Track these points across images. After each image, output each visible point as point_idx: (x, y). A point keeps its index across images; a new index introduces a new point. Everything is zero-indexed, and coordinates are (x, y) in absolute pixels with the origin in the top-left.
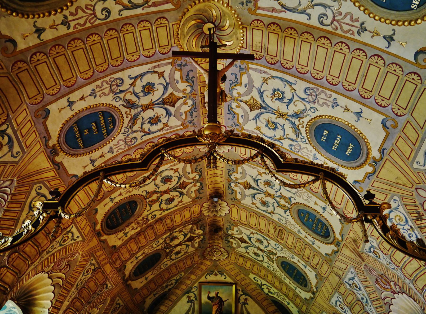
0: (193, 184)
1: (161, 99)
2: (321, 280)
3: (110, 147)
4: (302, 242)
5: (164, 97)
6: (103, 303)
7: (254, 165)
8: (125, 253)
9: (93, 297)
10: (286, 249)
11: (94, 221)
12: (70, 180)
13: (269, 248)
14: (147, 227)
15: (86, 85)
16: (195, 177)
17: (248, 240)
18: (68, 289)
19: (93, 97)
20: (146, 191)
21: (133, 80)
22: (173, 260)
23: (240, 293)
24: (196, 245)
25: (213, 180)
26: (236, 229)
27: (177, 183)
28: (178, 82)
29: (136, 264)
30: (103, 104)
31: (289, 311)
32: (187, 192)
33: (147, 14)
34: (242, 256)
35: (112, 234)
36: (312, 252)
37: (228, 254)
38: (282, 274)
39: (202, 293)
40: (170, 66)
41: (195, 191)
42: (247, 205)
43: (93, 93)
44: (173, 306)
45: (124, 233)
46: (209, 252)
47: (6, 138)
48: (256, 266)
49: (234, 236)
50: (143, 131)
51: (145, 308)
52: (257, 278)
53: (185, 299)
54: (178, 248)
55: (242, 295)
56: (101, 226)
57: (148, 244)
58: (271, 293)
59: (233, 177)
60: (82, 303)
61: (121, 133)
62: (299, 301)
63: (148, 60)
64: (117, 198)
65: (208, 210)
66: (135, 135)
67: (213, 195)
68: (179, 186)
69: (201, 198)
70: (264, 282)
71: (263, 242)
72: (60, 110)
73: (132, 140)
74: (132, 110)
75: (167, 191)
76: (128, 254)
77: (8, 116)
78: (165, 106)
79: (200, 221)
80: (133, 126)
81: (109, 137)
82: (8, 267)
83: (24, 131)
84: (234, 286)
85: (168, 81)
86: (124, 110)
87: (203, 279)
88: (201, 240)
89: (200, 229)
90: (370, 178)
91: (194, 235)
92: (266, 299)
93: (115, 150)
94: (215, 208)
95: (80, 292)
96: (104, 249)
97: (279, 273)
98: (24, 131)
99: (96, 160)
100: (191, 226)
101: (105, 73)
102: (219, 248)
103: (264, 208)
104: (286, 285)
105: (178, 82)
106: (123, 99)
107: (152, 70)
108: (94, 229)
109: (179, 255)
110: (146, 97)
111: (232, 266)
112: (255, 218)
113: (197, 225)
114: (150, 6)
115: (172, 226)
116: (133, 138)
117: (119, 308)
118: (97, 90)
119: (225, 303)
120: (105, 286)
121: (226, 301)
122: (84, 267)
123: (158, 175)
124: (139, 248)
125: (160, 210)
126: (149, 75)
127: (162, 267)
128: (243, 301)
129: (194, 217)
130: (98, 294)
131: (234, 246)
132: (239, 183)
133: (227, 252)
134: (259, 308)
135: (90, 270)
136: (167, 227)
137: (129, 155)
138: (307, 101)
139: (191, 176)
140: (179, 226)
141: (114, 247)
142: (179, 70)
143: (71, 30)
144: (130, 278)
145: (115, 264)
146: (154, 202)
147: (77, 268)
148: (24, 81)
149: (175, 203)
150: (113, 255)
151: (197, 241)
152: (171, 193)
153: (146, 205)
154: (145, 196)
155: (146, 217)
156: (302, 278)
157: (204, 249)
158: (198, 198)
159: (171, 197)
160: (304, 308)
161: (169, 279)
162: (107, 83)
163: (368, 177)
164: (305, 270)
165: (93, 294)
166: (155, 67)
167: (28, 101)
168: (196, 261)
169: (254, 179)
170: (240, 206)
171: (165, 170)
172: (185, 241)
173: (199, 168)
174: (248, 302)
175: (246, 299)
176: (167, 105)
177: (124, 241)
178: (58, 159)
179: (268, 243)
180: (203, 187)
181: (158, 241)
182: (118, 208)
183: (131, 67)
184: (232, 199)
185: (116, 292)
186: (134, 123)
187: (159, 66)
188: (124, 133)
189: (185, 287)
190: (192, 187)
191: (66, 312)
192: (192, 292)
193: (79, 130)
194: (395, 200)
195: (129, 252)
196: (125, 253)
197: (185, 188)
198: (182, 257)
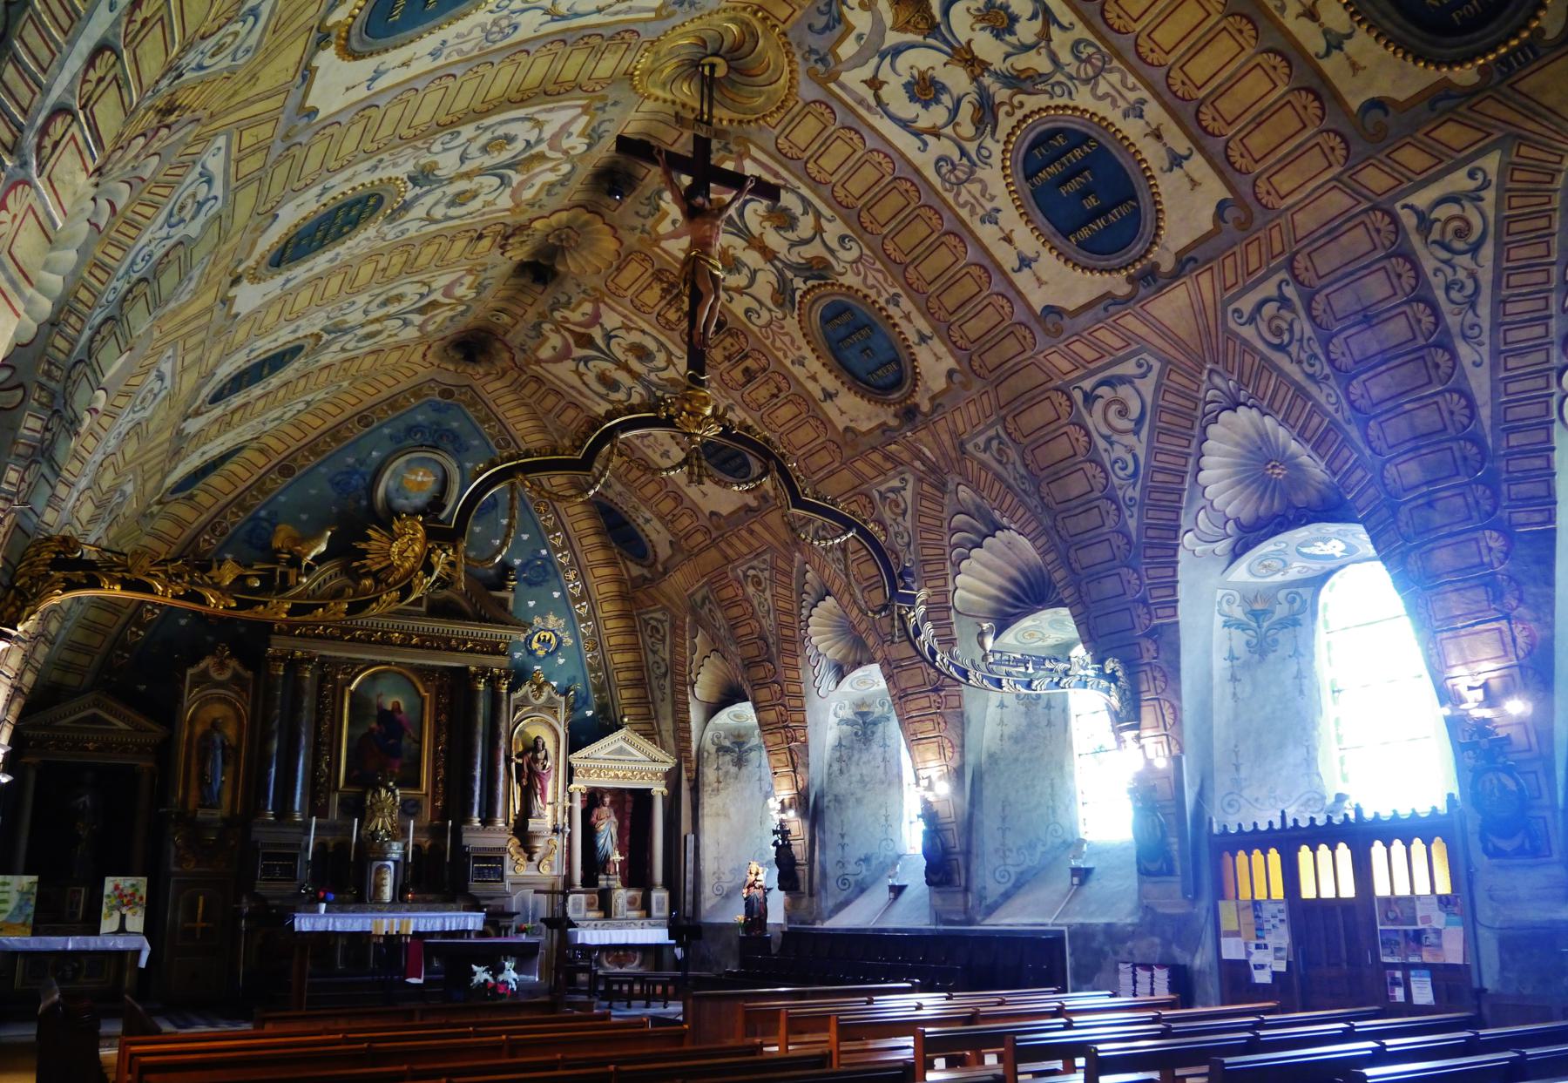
1: (930, 41)
3: (1126, 115)
5: (920, 38)
12: (1231, 225)
15: (978, 240)
21: (926, 137)
28: (860, 37)
30: (1007, 185)
33: (799, 179)
40: (844, 77)
43: (991, 218)
50: (1045, 36)
61: (1071, 104)
63: (865, 132)
66: (1065, 57)
73: (1084, 56)
74: (997, 100)
77: (1057, 389)
78: (938, 18)
80: (1040, 75)
81: (1094, 134)
82: (1389, 460)
83: (1089, 354)
85: (876, 60)
86: (1005, 124)
93: (1132, 96)
98: (1089, 354)
99: (1170, 151)
101: (938, 208)
105: (860, 37)
108: (1471, 92)
110: (948, 83)
116: (1077, 58)
118: (980, 211)
126: (892, 108)
137: (1136, 45)
142: (836, 56)
143: (898, 290)
148: (997, 361)
162: (958, 194)
166: (869, 108)
167: (1029, 354)
176: (932, 17)
178: (1167, 265)
183: (902, 155)
186: (1030, 77)
187: (861, 102)
188: (1070, 93)
193: (1085, 224)
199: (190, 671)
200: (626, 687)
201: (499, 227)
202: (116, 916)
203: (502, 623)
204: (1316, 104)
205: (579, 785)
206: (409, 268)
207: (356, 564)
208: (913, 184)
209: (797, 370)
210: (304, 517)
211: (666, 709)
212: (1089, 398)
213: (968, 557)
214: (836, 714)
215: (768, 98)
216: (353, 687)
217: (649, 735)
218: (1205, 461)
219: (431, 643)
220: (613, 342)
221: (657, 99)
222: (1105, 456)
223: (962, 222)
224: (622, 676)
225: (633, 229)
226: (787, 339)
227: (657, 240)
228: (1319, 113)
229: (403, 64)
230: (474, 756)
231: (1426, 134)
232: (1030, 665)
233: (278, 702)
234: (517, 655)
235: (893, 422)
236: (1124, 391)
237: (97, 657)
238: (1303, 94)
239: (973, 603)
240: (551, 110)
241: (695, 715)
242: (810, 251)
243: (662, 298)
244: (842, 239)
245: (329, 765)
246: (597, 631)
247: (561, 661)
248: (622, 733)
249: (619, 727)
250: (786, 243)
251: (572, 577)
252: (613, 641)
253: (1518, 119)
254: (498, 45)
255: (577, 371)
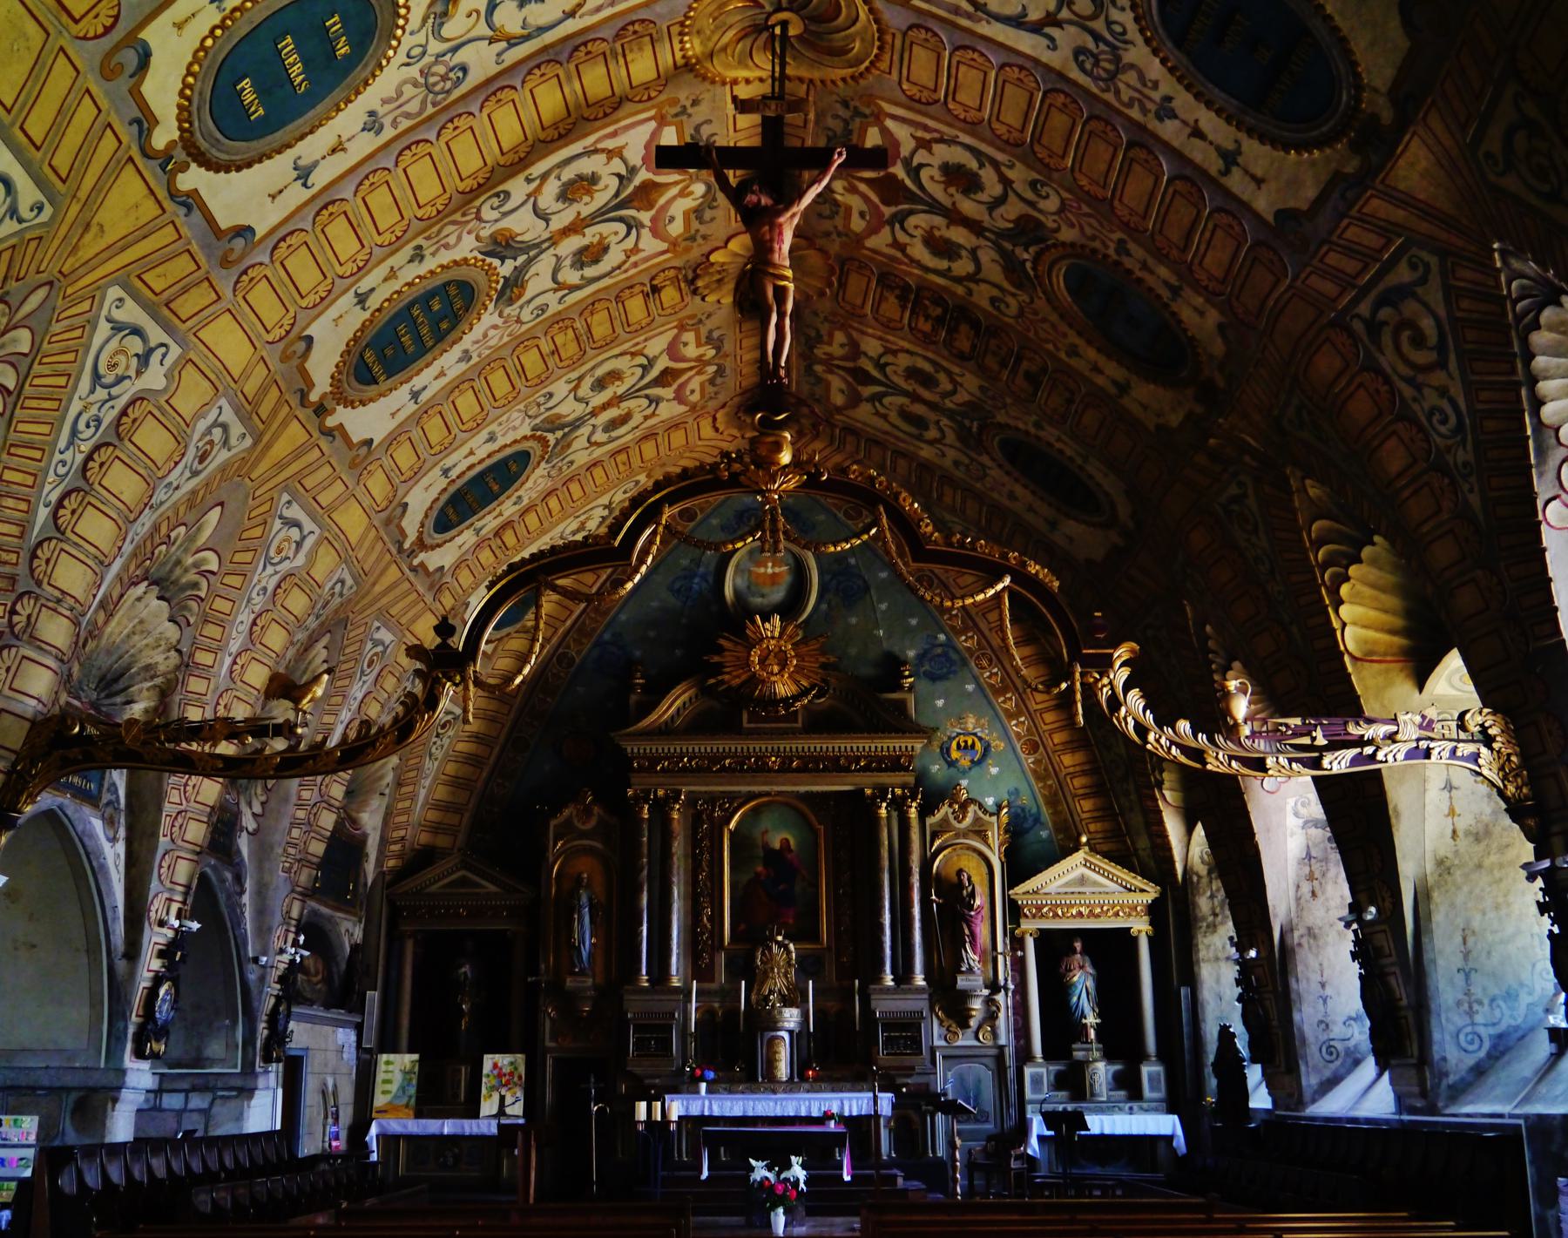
15: (1166, 146)
19: (1174, 104)
21: (1048, 30)
30: (1163, 62)
43: (1166, 111)
47: (1385, 313)
72: (1259, 182)
83: (1351, 266)
90: (135, 127)
98: (1351, 266)
106: (1102, 18)
107: (979, 13)
114: (936, 131)
138: (444, 55)
162: (1117, 92)
163: (138, 122)
166: (969, 16)
183: (1036, 61)
194: (40, 209)
199: (553, 823)
200: (1085, 796)
201: (672, 273)
202: (496, 1097)
203: (897, 731)
205: (1028, 926)
206: (587, 343)
207: (712, 681)
208: (1067, 95)
209: (1074, 362)
210: (652, 634)
211: (1137, 819)
212: (1374, 327)
213: (1347, 579)
214: (1296, 814)
215: (863, 40)
216: (732, 825)
217: (1122, 857)
218: (1545, 387)
219: (811, 765)
220: (888, 369)
221: (748, 81)
222: (1416, 407)
223: (1142, 128)
224: (1078, 782)
225: (828, 234)
226: (1045, 326)
227: (859, 240)
229: (334, 151)
230: (881, 898)
232: (1318, 734)
233: (645, 850)
234: (935, 768)
235: (1199, 409)
236: (1410, 308)
237: (467, 815)
239: (1375, 642)
240: (614, 134)
241: (1173, 827)
242: (1013, 209)
243: (904, 308)
244: (1033, 185)
245: (710, 919)
246: (1034, 727)
247: (994, 770)
248: (1079, 856)
249: (1077, 850)
250: (983, 208)
251: (985, 663)
252: (1057, 738)
254: (456, 94)
255: (877, 413)
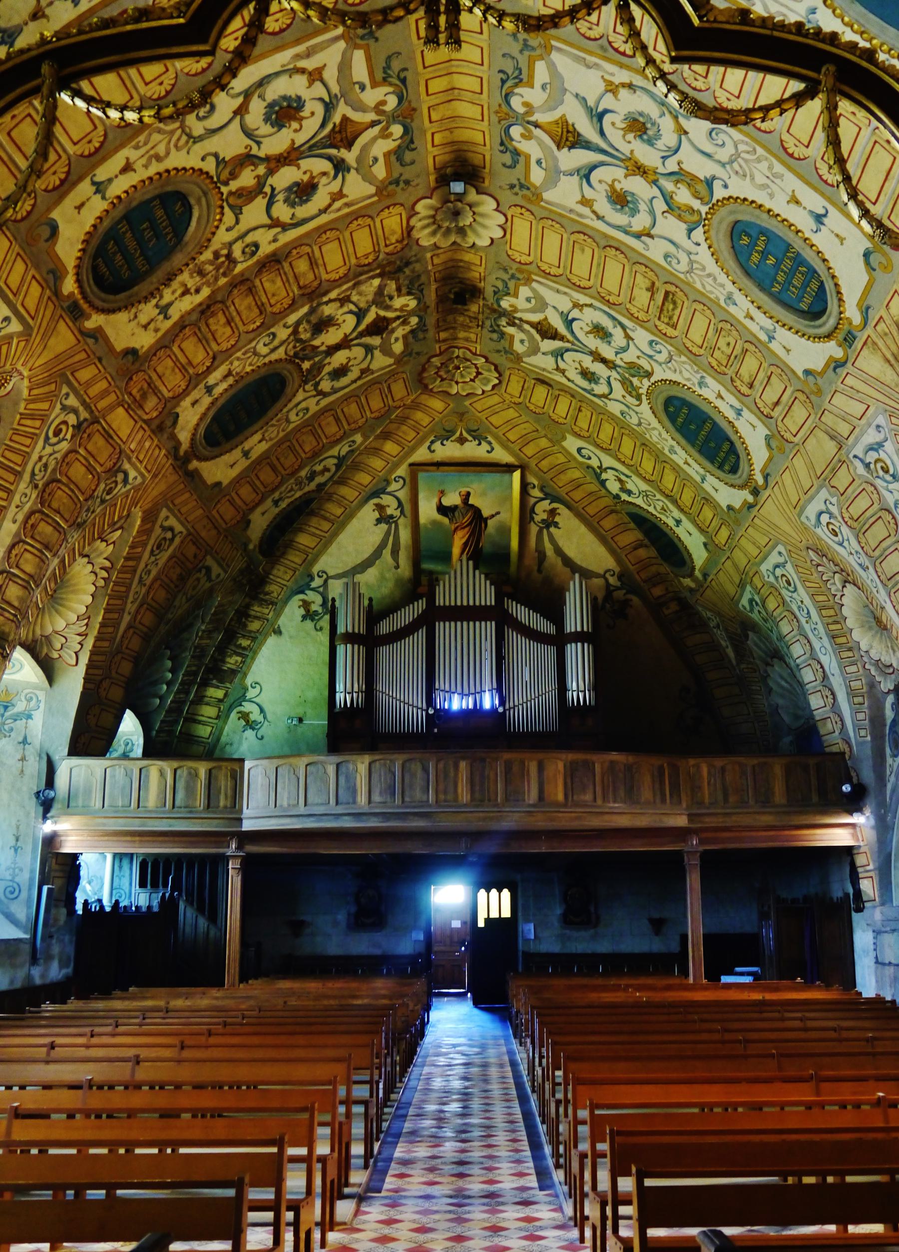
0: (377, 129)
2: (781, 450)
4: (734, 332)
6: (121, 528)
7: (591, 53)
8: (168, 372)
9: (88, 510)
10: (683, 358)
11: (52, 266)
13: (631, 356)
14: (233, 285)
16: (383, 103)
17: (562, 330)
18: (7, 485)
20: (216, 155)
22: (325, 395)
23: (536, 493)
24: (398, 348)
25: (449, 114)
26: (524, 291)
27: (323, 125)
29: (208, 409)
31: (680, 545)
32: (359, 160)
34: (542, 381)
35: (120, 310)
36: (765, 365)
37: (500, 375)
38: (665, 435)
39: (421, 496)
41: (387, 155)
42: (563, 207)
44: (335, 534)
45: (157, 306)
46: (439, 369)
48: (586, 413)
49: (518, 315)
51: (249, 540)
52: (589, 449)
53: (368, 514)
54: (340, 358)
55: (542, 499)
56: (78, 281)
57: (240, 344)
58: (629, 493)
59: (516, 103)
60: (57, 527)
62: (711, 516)
64: (115, 181)
65: (434, 227)
67: (449, 171)
68: (329, 136)
69: (407, 182)
70: (608, 461)
71: (611, 335)
75: (290, 157)
76: (179, 376)
79: (407, 264)
84: (517, 475)
87: (421, 454)
88: (412, 331)
89: (409, 294)
91: (390, 315)
92: (612, 512)
94: (457, 221)
95: (46, 495)
96: (100, 360)
97: (656, 433)
100: (376, 282)
102: (469, 355)
103: (621, 219)
104: (676, 469)
108: (57, 292)
109: (344, 381)
111: (511, 413)
112: (588, 252)
113: (397, 280)
115: (316, 284)
117: (172, 540)
119: (490, 522)
120: (120, 477)
121: (493, 516)
122: (43, 418)
123: (252, 94)
124: (214, 358)
125: (270, 227)
127: (293, 417)
128: (544, 516)
129: (388, 250)
130: (103, 501)
131: (518, 348)
132: (536, 125)
133: (496, 369)
134: (590, 538)
135: (64, 427)
136: (300, 287)
139: (371, 97)
140: (336, 283)
141: (132, 352)
144: (194, 453)
145: (141, 407)
146: (247, 195)
147: (23, 422)
149: (320, 199)
150: (131, 379)
151: (400, 332)
152: (305, 164)
153: (222, 207)
154: (213, 172)
155: (225, 252)
156: (726, 447)
157: (423, 359)
158: (397, 182)
159: (306, 178)
160: (724, 533)
161: (315, 455)
164: (736, 424)
165: (86, 500)
168: (397, 396)
169: (590, 111)
170: (539, 213)
171: (277, 74)
172: (361, 335)
173: (396, 65)
174: (557, 519)
175: (553, 512)
177: (160, 334)
179: (628, 337)
180: (412, 142)
181: (274, 335)
182: (126, 217)
184: (512, 187)
185: (155, 493)
189: (369, 478)
190: (374, 140)
191: (14, 552)
192: (389, 494)
195: (183, 369)
196: (168, 372)
197: (349, 145)
198: (354, 386)
204: (58, 182)
228: (50, 187)
231: (34, 277)
238: (66, 169)
253: (42, 330)
